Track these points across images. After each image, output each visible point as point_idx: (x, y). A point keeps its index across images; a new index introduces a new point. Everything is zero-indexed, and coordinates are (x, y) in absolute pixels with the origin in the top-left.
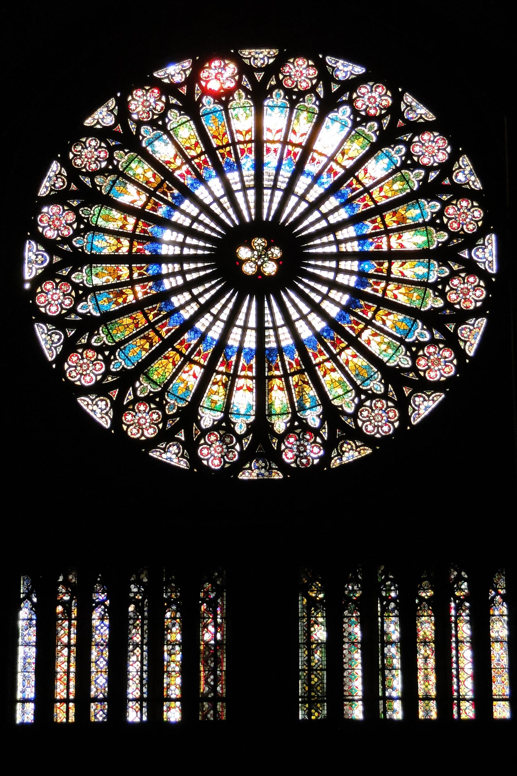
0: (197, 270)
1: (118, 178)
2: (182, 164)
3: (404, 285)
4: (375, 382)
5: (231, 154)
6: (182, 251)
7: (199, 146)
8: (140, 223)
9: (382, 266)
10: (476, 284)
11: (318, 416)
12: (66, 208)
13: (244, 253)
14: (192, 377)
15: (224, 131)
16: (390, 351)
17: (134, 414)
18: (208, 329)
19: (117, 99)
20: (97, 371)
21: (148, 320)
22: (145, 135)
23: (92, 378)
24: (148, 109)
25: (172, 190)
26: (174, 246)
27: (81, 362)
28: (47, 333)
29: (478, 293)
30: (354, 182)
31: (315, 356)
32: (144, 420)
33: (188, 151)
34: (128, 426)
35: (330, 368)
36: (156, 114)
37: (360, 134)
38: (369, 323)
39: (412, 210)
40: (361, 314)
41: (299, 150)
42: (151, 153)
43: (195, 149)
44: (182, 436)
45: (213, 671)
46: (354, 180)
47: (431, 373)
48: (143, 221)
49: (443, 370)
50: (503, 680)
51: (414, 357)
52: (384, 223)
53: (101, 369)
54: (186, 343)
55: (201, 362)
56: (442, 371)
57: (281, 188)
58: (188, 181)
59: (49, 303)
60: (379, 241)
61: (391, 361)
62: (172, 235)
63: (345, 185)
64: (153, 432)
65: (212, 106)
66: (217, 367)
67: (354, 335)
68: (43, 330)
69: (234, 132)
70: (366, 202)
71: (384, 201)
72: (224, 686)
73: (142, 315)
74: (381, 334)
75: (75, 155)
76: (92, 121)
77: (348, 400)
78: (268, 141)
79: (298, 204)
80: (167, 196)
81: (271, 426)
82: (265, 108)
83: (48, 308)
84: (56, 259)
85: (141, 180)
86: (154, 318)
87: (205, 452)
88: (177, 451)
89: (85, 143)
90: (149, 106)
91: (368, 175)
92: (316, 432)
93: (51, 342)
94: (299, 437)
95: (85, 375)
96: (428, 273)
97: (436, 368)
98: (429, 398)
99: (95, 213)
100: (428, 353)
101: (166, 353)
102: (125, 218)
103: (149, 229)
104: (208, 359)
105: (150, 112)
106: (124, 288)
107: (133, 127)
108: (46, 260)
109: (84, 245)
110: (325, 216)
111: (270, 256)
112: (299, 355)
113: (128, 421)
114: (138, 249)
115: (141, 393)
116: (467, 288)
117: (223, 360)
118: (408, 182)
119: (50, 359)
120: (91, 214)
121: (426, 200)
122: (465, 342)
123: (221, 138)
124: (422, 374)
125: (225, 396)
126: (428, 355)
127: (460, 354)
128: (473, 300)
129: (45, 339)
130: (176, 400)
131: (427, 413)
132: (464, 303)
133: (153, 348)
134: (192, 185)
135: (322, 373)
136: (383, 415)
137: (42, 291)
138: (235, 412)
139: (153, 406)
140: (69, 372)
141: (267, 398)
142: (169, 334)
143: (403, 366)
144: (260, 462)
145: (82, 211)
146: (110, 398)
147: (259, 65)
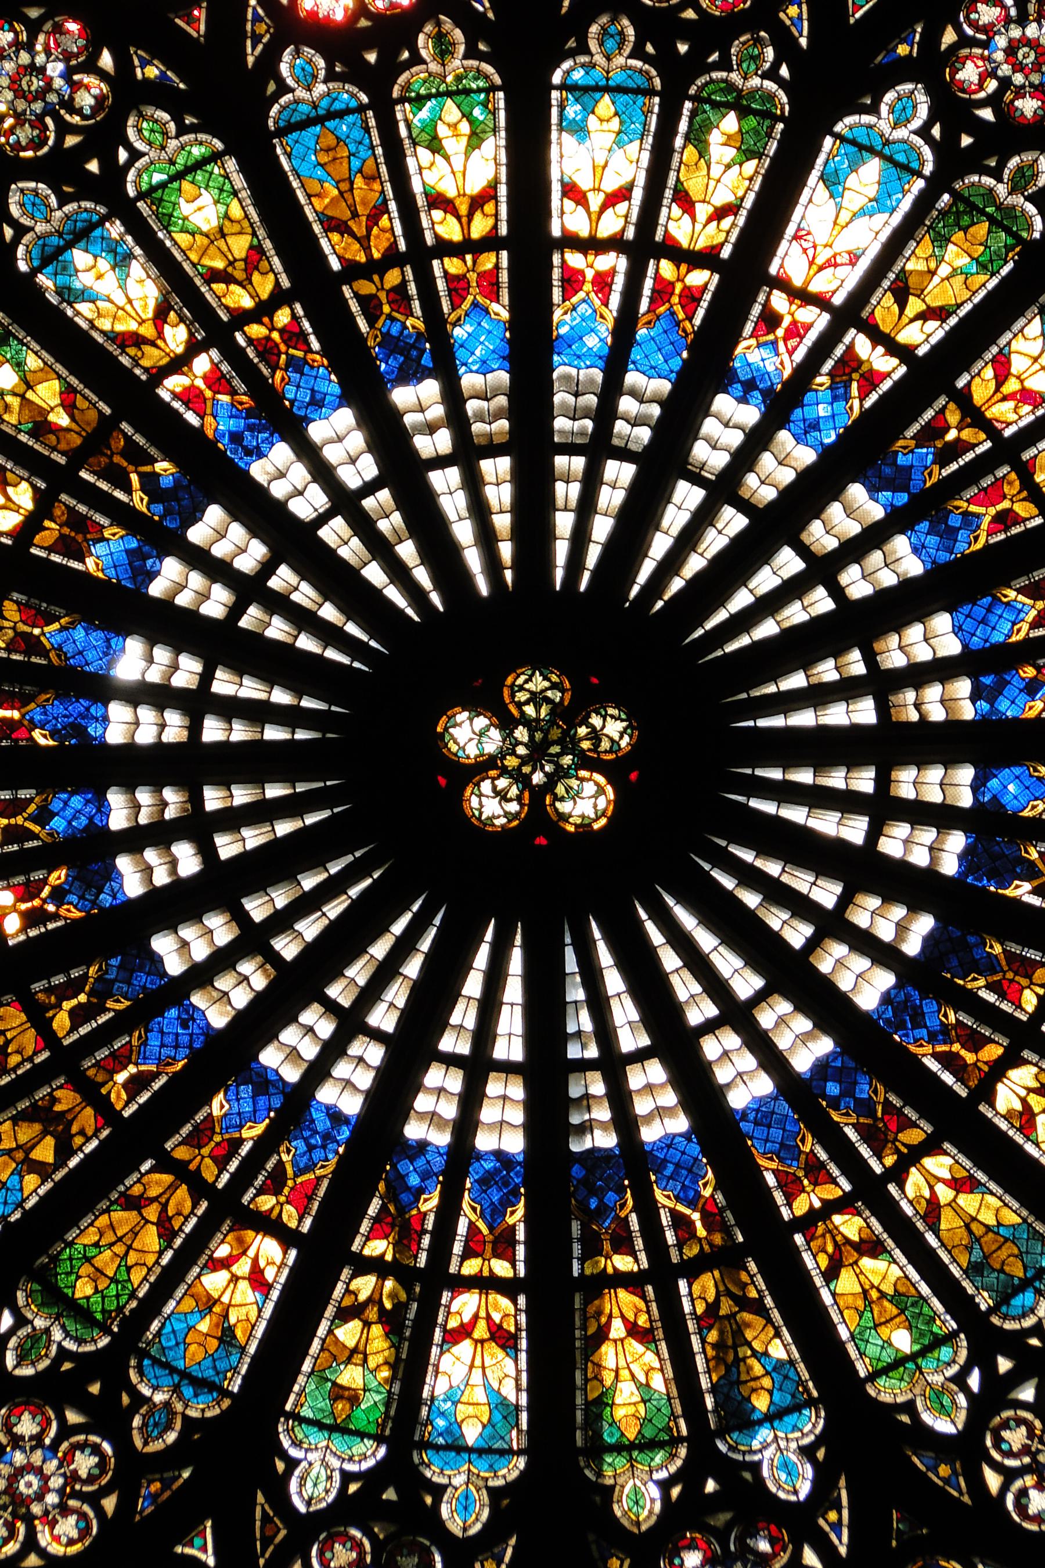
2: (193, 348)
5: (409, 299)
6: (195, 728)
7: (264, 265)
11: (807, 1452)
14: (244, 1285)
15: (374, 197)
21: (47, 1035)
22: (26, 221)
24: (38, 106)
25: (153, 461)
26: (160, 708)
30: (953, 417)
31: (791, 1188)
33: (219, 287)
35: (856, 1238)
36: (74, 130)
37: (972, 207)
40: (990, 997)
42: (54, 299)
44: (204, 1549)
46: (952, 406)
48: (23, 598)
54: (217, 1138)
57: (632, 446)
62: (150, 660)
63: (911, 432)
64: (74, 1534)
65: (320, 88)
66: (358, 1241)
67: (963, 1093)
69: (421, 201)
70: (1005, 504)
73: (23, 1017)
77: (937, 1379)
78: (571, 241)
82: (555, 95)
85: (12, 418)
86: (74, 1028)
90: (41, 95)
91: (1012, 386)
94: (725, 1546)
101: (128, 1182)
103: (50, 633)
105: (49, 121)
111: (586, 745)
115: (21, 1360)
117: (383, 1208)
123: (360, 230)
130: (176, 1389)
133: (73, 1163)
134: (236, 438)
135: (823, 1261)
138: (441, 1441)
139: (73, 1417)
141: (578, 1376)
142: (143, 1098)
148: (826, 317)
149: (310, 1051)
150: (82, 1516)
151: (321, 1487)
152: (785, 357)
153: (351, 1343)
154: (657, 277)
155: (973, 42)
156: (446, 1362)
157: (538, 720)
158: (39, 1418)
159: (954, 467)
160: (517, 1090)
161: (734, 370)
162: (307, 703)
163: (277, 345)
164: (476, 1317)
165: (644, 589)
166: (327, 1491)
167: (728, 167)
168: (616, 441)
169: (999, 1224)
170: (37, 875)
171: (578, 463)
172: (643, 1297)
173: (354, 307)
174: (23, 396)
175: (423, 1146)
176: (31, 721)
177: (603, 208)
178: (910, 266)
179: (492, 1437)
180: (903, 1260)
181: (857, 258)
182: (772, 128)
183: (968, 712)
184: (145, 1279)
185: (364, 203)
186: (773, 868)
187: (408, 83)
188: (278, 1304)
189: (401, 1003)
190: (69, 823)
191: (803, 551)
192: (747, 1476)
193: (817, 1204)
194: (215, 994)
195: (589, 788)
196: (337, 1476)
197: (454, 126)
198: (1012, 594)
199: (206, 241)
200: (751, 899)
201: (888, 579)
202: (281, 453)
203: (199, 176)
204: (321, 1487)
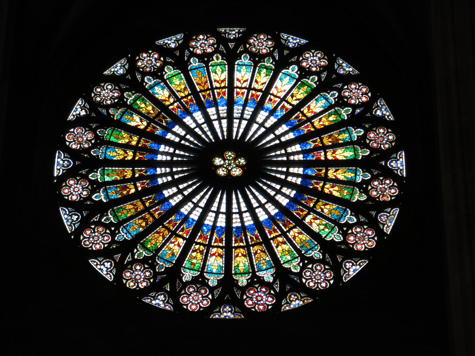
0: (182, 172)
1: (126, 110)
2: (174, 102)
3: (337, 185)
4: (316, 252)
7: (187, 90)
8: (142, 141)
9: (321, 171)
11: (272, 275)
14: (176, 246)
15: (205, 80)
16: (327, 230)
17: (132, 272)
18: (190, 213)
19: (128, 59)
20: (105, 241)
22: (148, 82)
23: (101, 245)
24: (150, 65)
25: (167, 119)
26: (166, 156)
27: (93, 235)
28: (69, 214)
29: (393, 191)
30: (301, 115)
31: (271, 233)
32: (139, 277)
33: (179, 93)
34: (127, 280)
35: (281, 241)
37: (305, 84)
38: (311, 210)
39: (344, 134)
41: (260, 94)
43: (184, 92)
46: (300, 113)
47: (358, 246)
48: (144, 139)
49: (367, 244)
51: (345, 234)
52: (322, 142)
53: (108, 240)
54: (173, 223)
55: (184, 236)
56: (366, 245)
58: (179, 112)
59: (71, 193)
60: (319, 155)
61: (328, 237)
65: (197, 64)
68: (66, 212)
69: (213, 81)
70: (309, 128)
73: (141, 203)
74: (320, 218)
75: (95, 95)
76: (109, 72)
78: (237, 87)
81: (236, 282)
82: (236, 66)
87: (185, 299)
88: (164, 299)
89: (103, 87)
90: (151, 64)
91: (310, 111)
92: (269, 286)
93: (71, 221)
94: (257, 290)
95: (96, 244)
96: (355, 176)
97: (362, 243)
99: (109, 133)
100: (356, 232)
101: (157, 229)
102: (131, 137)
103: (148, 144)
104: (189, 234)
105: (152, 68)
106: (128, 184)
107: (139, 77)
109: (100, 154)
110: (278, 137)
111: (238, 163)
112: (258, 232)
114: (139, 158)
116: (384, 188)
117: (201, 235)
118: (340, 116)
119: (70, 232)
120: (106, 134)
121: (353, 128)
122: (384, 225)
123: (203, 85)
125: (202, 260)
126: (355, 233)
127: (380, 233)
128: (389, 196)
129: (66, 219)
130: (164, 262)
132: (382, 197)
134: (181, 115)
135: (276, 245)
136: (322, 275)
137: (66, 185)
138: (209, 272)
139: (146, 266)
140: (84, 242)
143: (337, 240)
144: (227, 307)
146: (115, 261)
148: (280, 100)
150: (147, 282)
151: (188, 279)
152: (273, 106)
153: (194, 256)
154: (252, 93)
155: (305, 59)
157: (230, 159)
158: (140, 266)
160: (224, 216)
161: (264, 107)
163: (188, 102)
164: (216, 252)
165: (248, 140)
166: (189, 279)
167: (264, 77)
168: (244, 117)
169: (306, 240)
171: (238, 121)
172: (245, 250)
173: (201, 96)
174: (146, 108)
175: (208, 225)
176: (145, 157)
177: (243, 82)
178: (294, 93)
179: (218, 271)
180: (289, 245)
181: (285, 91)
182: (271, 71)
183: (302, 159)
184: (160, 245)
185: (204, 81)
186: (269, 183)
187: (212, 63)
188: (182, 249)
189: (205, 202)
190: (150, 173)
193: (275, 236)
194: (174, 200)
195: (238, 170)
196: (191, 277)
197: (219, 70)
198: (310, 142)
199: (177, 86)
200: (265, 188)
203: (177, 76)
204: (188, 279)
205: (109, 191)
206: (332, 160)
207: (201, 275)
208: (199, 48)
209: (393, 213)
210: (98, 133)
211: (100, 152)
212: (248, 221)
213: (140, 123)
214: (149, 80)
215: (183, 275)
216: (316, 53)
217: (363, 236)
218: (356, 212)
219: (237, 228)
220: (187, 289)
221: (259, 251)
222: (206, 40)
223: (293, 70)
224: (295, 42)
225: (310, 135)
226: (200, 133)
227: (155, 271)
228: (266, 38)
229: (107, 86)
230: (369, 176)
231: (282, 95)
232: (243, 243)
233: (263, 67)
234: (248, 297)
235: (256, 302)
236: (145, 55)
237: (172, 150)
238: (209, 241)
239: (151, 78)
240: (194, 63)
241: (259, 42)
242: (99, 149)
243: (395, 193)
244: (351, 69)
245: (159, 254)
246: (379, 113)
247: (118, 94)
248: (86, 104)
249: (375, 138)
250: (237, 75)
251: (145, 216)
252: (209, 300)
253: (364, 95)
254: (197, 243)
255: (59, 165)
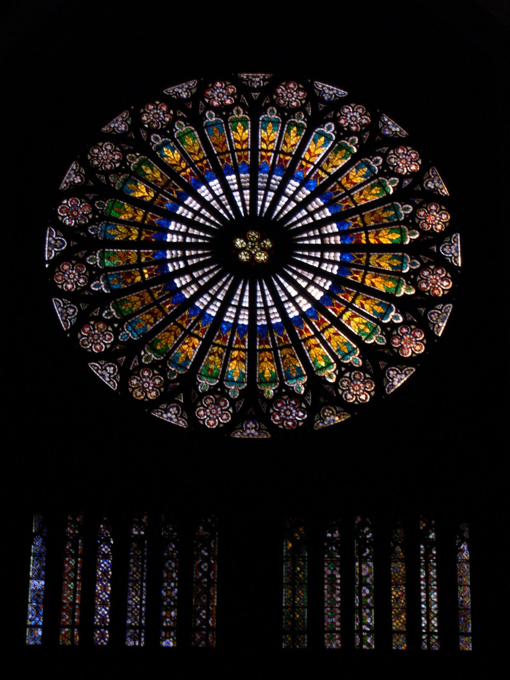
0: (197, 256)
2: (187, 167)
3: (381, 274)
4: (354, 357)
6: (184, 239)
8: (149, 216)
10: (444, 275)
12: (83, 200)
13: (239, 243)
14: (191, 348)
15: (224, 140)
17: (139, 378)
18: (207, 307)
22: (155, 142)
25: (178, 188)
26: (178, 235)
30: (338, 187)
33: (193, 156)
34: (133, 389)
38: (349, 306)
39: (388, 212)
40: (342, 298)
45: (206, 606)
50: (466, 619)
52: (363, 221)
56: (413, 349)
59: (66, 281)
62: (176, 226)
67: (336, 316)
68: (60, 304)
69: (233, 141)
70: (347, 204)
71: (363, 202)
72: (215, 620)
74: (360, 315)
76: (108, 129)
78: (263, 150)
79: (287, 203)
80: (173, 193)
82: (260, 123)
83: (64, 285)
84: (73, 243)
86: (158, 297)
87: (202, 413)
88: (176, 412)
89: (101, 147)
91: (350, 181)
92: (300, 398)
95: (96, 344)
96: (402, 265)
97: (409, 346)
98: (401, 372)
100: (401, 333)
102: (135, 211)
103: (155, 221)
104: (206, 333)
105: (160, 123)
107: (144, 134)
108: (64, 244)
109: (99, 232)
111: (263, 246)
113: (134, 385)
114: (146, 237)
115: (145, 361)
117: (220, 334)
119: (65, 329)
122: (434, 325)
123: (221, 146)
124: (396, 350)
125: (221, 365)
126: (401, 334)
130: (177, 368)
131: (399, 385)
133: (157, 323)
134: (195, 184)
137: (60, 271)
139: (156, 372)
142: (172, 311)
144: (251, 423)
145: (97, 204)
147: (255, 86)
148: (312, 167)
149: (205, 303)
150: (157, 392)
154: (280, 158)
155: (343, 116)
156: (231, 364)
159: (337, 196)
160: (247, 313)
162: (207, 235)
164: (237, 356)
170: (152, 267)
171: (263, 192)
172: (271, 353)
173: (219, 161)
175: (228, 322)
178: (330, 157)
183: (339, 242)
186: (300, 271)
189: (224, 295)
191: (307, 210)
192: (291, 389)
196: (208, 386)
200: (295, 277)
201: (324, 216)
202: (203, 187)
205: (111, 279)
206: (375, 244)
207: (220, 385)
208: (216, 98)
209: (445, 310)
210: (96, 205)
211: (99, 230)
212: (276, 319)
213: (146, 194)
214: (156, 139)
215: (200, 383)
216: (356, 107)
217: (410, 339)
218: (402, 310)
219: (262, 326)
220: (203, 400)
221: (288, 356)
222: (225, 89)
223: (329, 129)
224: (331, 93)
225: (350, 212)
226: (217, 207)
227: (165, 377)
228: (297, 87)
229: (106, 146)
230: (417, 264)
231: (317, 160)
232: (269, 345)
233: (293, 124)
234: (274, 411)
235: (284, 417)
236: (151, 107)
237: (183, 228)
238: (229, 343)
239: (158, 136)
240: (211, 118)
241: (288, 93)
242: (98, 226)
243: (448, 285)
244: (398, 130)
245: (171, 357)
246: (430, 185)
247: (119, 157)
248: (82, 169)
249: (425, 217)
250: (262, 134)
251: (153, 310)
252: (230, 415)
253: (413, 163)
254: (215, 345)
255: (51, 246)
